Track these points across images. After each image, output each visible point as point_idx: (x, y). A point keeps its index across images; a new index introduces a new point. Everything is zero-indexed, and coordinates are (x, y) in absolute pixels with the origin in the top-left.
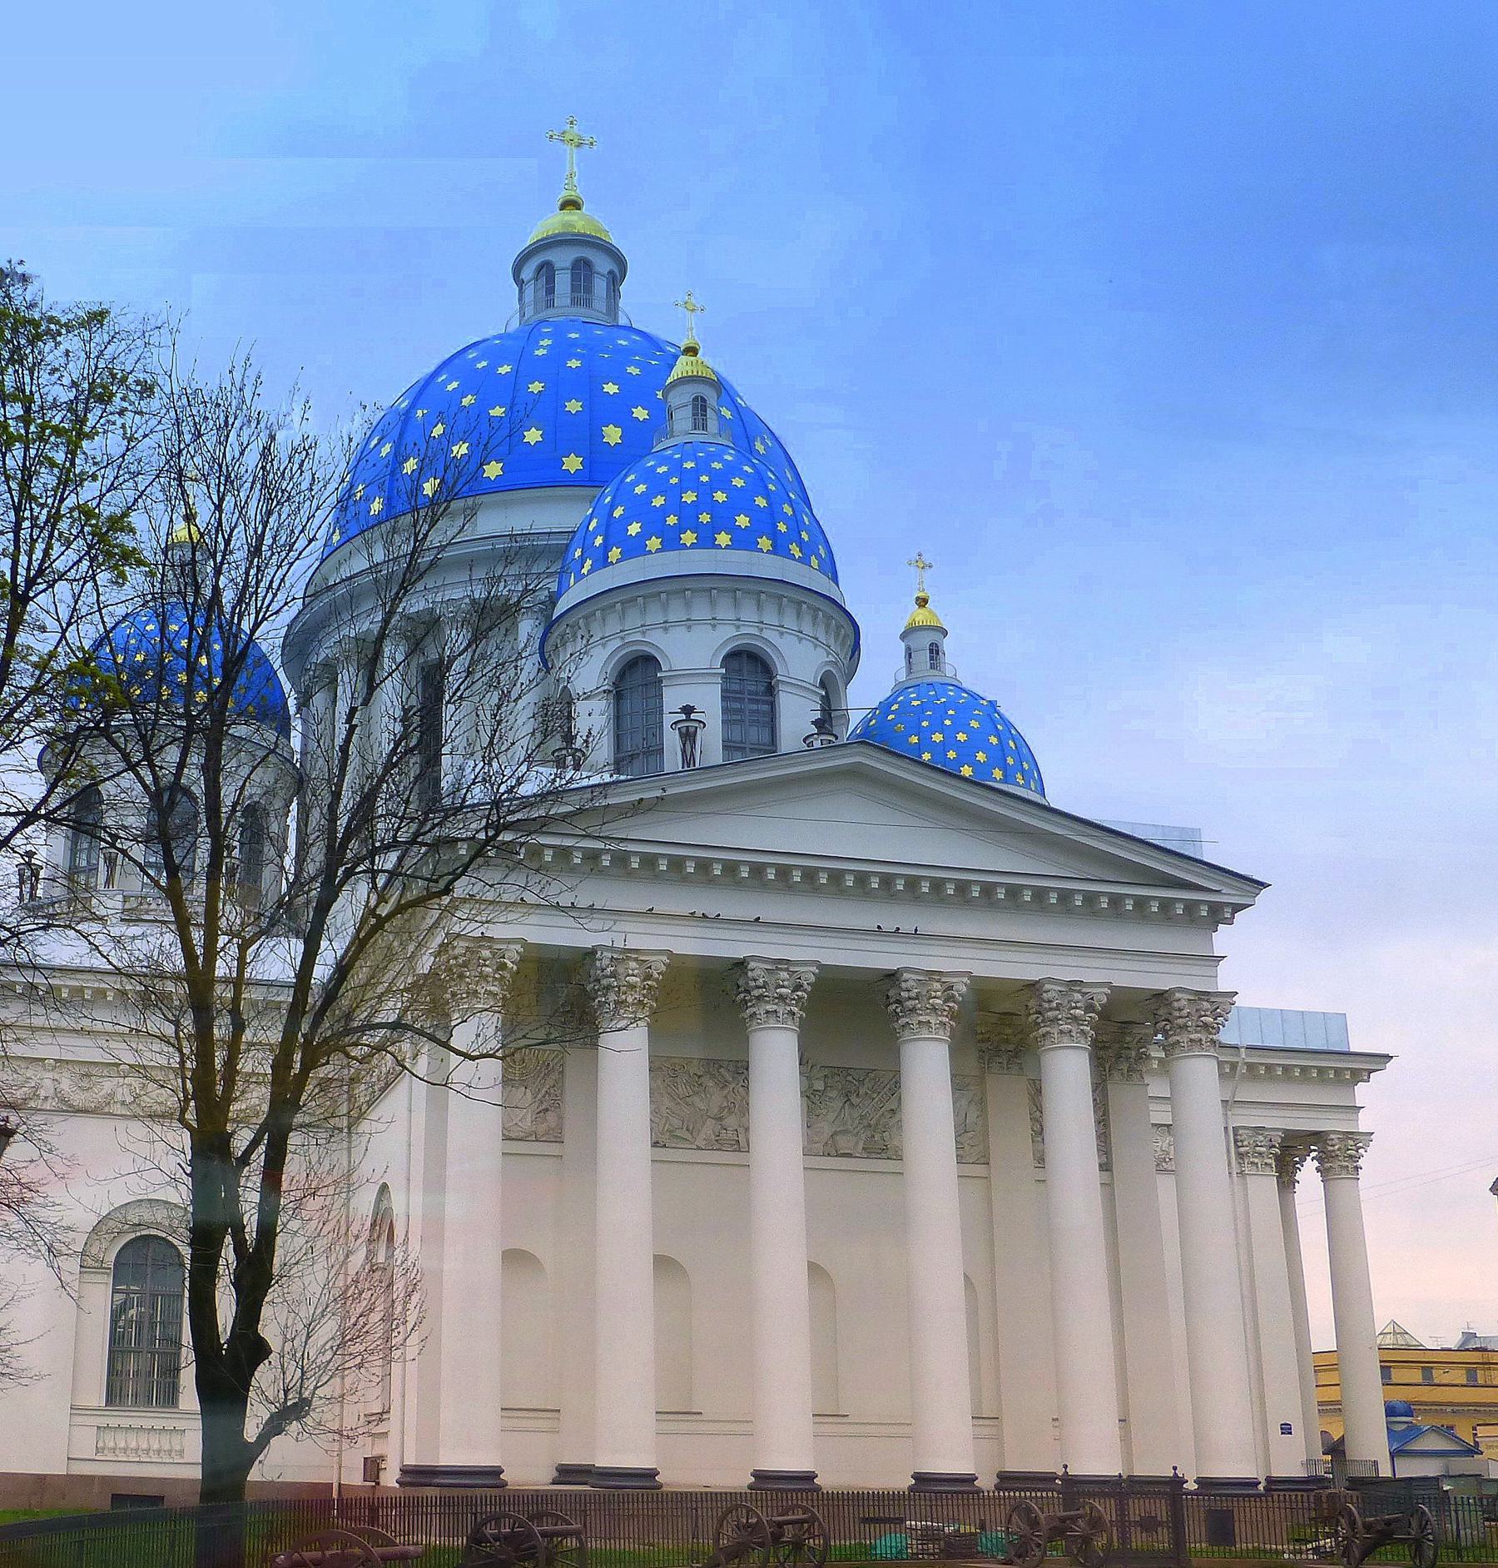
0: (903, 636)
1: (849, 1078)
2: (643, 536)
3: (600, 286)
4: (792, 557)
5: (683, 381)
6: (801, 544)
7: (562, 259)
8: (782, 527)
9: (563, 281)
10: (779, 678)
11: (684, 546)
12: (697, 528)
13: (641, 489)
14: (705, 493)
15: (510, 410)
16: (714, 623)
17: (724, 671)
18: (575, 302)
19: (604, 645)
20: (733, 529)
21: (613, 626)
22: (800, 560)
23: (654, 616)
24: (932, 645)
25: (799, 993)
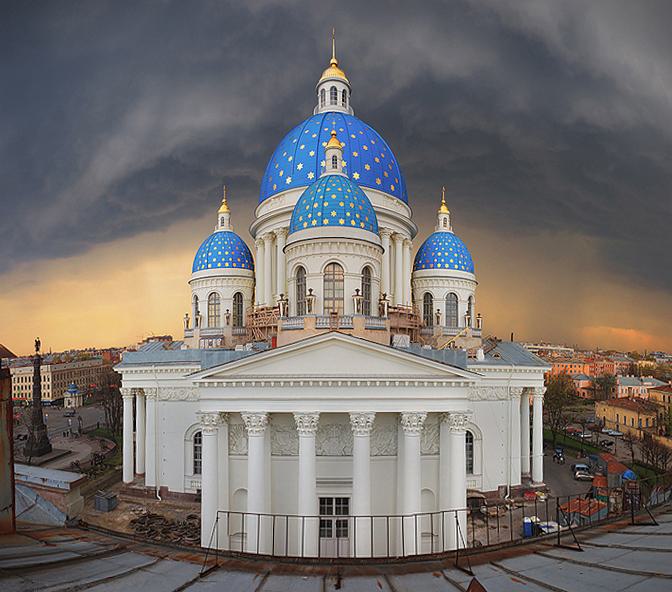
8: (348, 214)
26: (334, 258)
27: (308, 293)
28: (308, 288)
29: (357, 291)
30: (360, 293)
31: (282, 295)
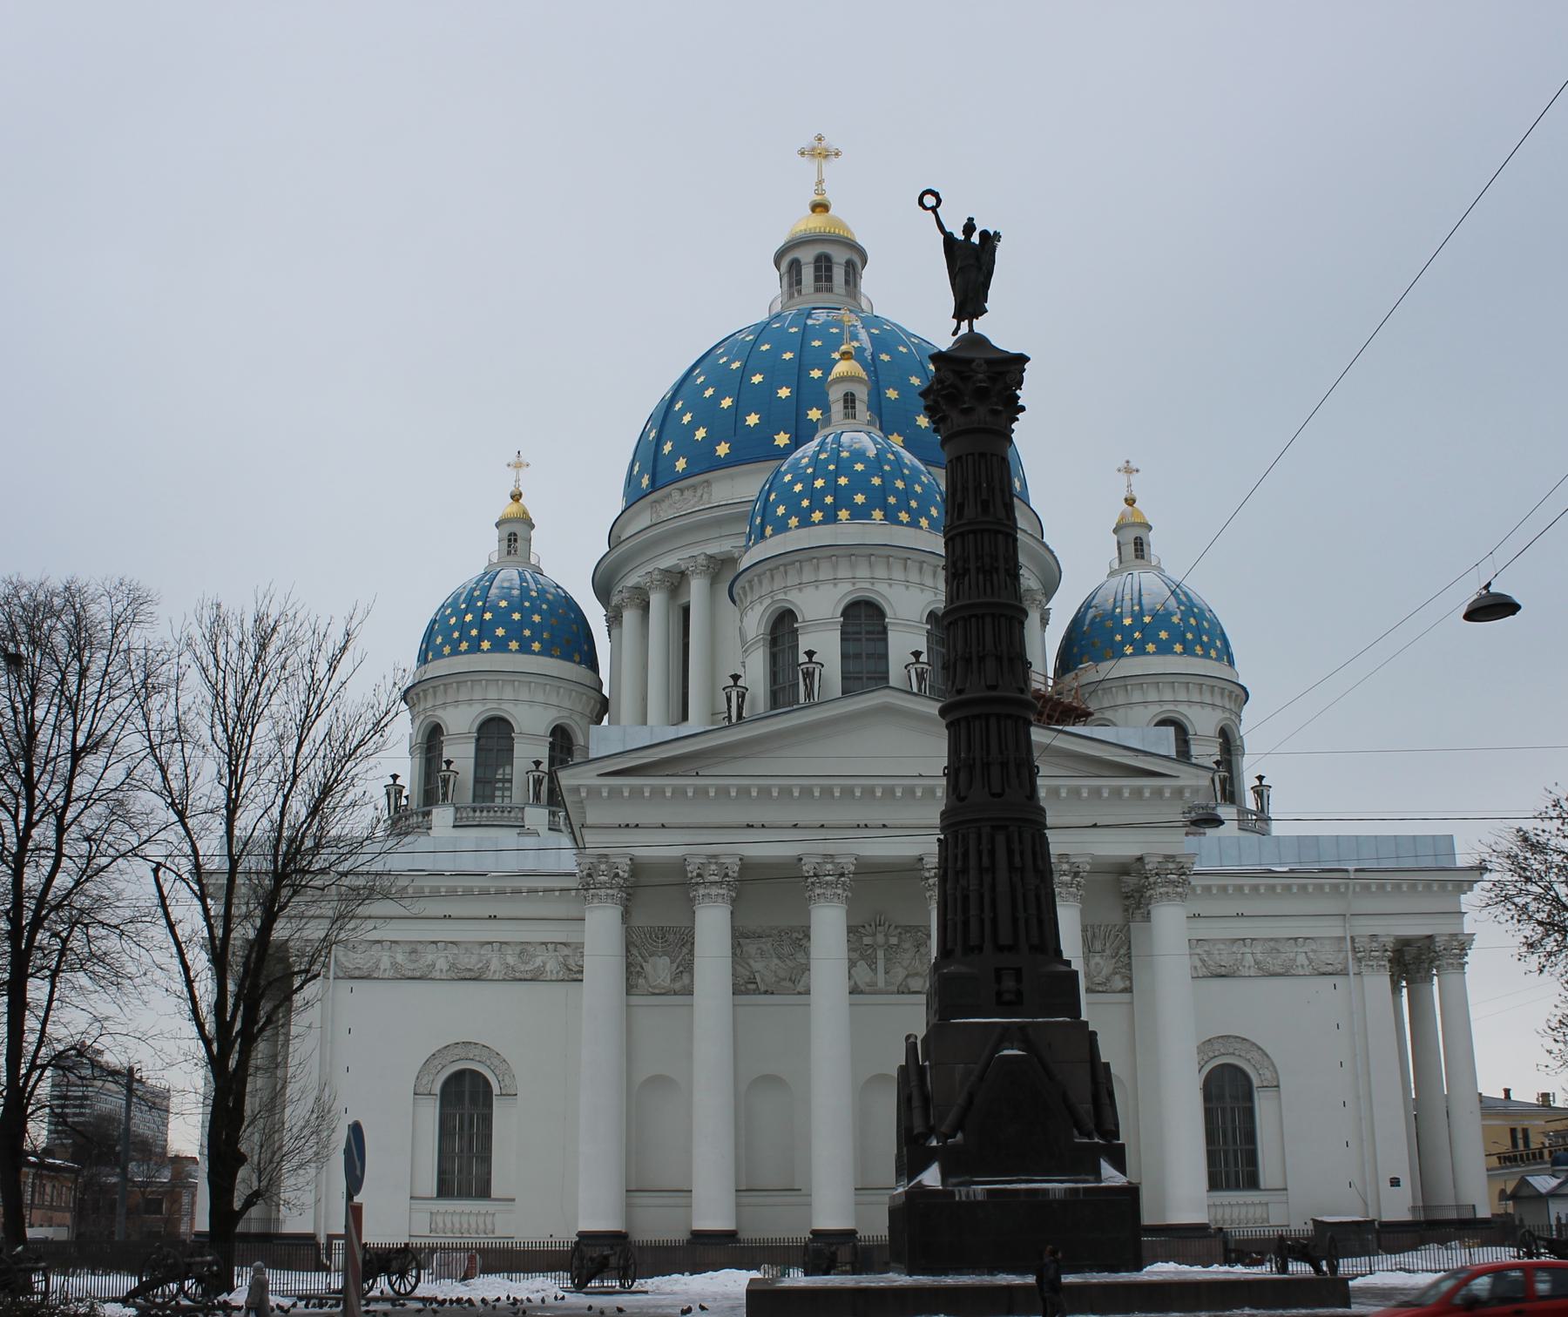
0: (1115, 531)
1: (920, 934)
2: (787, 516)
3: (839, 274)
5: (842, 379)
6: (909, 511)
7: (807, 256)
8: (892, 500)
9: (808, 274)
10: (887, 620)
11: (814, 524)
12: (823, 507)
15: (736, 403)
16: (835, 581)
17: (842, 619)
18: (818, 290)
19: (761, 603)
21: (766, 588)
22: (908, 524)
23: (792, 580)
24: (1136, 539)
25: (843, 879)
26: (863, 590)
27: (803, 658)
28: (802, 648)
29: (917, 654)
30: (924, 658)
31: (736, 677)
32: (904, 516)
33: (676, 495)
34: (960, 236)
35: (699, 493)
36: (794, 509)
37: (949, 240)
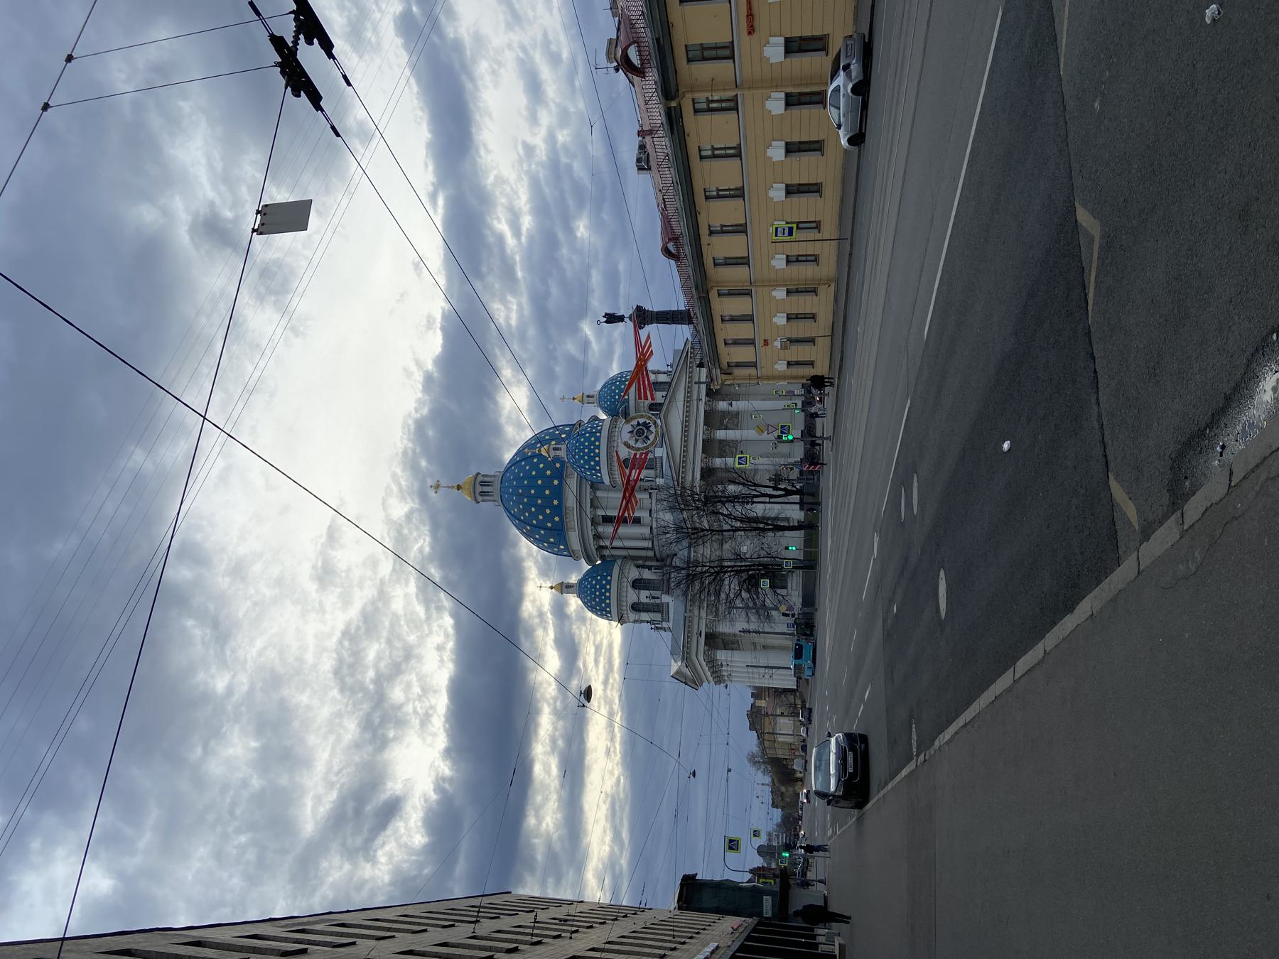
4: (601, 429)
7: (479, 489)
9: (486, 489)
13: (582, 462)
14: (585, 447)
20: (595, 441)
32: (599, 428)
33: (567, 520)
34: (605, 319)
35: (568, 511)
36: (593, 459)
37: (606, 322)
